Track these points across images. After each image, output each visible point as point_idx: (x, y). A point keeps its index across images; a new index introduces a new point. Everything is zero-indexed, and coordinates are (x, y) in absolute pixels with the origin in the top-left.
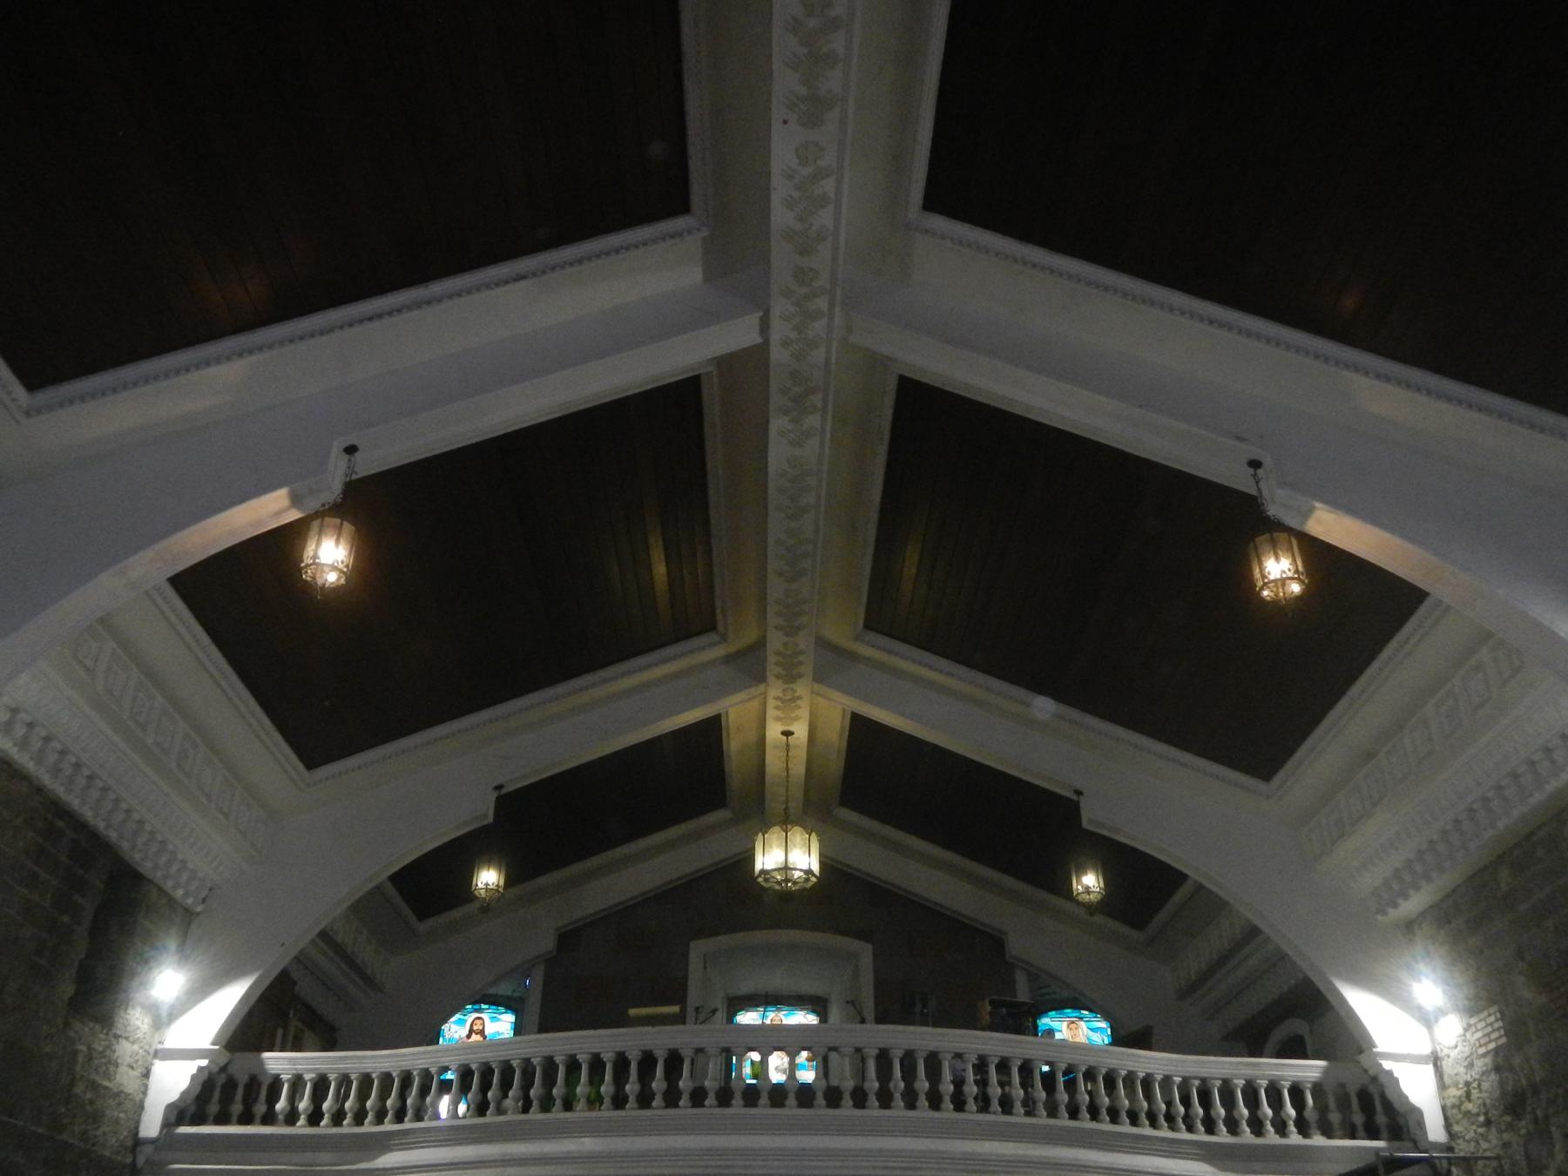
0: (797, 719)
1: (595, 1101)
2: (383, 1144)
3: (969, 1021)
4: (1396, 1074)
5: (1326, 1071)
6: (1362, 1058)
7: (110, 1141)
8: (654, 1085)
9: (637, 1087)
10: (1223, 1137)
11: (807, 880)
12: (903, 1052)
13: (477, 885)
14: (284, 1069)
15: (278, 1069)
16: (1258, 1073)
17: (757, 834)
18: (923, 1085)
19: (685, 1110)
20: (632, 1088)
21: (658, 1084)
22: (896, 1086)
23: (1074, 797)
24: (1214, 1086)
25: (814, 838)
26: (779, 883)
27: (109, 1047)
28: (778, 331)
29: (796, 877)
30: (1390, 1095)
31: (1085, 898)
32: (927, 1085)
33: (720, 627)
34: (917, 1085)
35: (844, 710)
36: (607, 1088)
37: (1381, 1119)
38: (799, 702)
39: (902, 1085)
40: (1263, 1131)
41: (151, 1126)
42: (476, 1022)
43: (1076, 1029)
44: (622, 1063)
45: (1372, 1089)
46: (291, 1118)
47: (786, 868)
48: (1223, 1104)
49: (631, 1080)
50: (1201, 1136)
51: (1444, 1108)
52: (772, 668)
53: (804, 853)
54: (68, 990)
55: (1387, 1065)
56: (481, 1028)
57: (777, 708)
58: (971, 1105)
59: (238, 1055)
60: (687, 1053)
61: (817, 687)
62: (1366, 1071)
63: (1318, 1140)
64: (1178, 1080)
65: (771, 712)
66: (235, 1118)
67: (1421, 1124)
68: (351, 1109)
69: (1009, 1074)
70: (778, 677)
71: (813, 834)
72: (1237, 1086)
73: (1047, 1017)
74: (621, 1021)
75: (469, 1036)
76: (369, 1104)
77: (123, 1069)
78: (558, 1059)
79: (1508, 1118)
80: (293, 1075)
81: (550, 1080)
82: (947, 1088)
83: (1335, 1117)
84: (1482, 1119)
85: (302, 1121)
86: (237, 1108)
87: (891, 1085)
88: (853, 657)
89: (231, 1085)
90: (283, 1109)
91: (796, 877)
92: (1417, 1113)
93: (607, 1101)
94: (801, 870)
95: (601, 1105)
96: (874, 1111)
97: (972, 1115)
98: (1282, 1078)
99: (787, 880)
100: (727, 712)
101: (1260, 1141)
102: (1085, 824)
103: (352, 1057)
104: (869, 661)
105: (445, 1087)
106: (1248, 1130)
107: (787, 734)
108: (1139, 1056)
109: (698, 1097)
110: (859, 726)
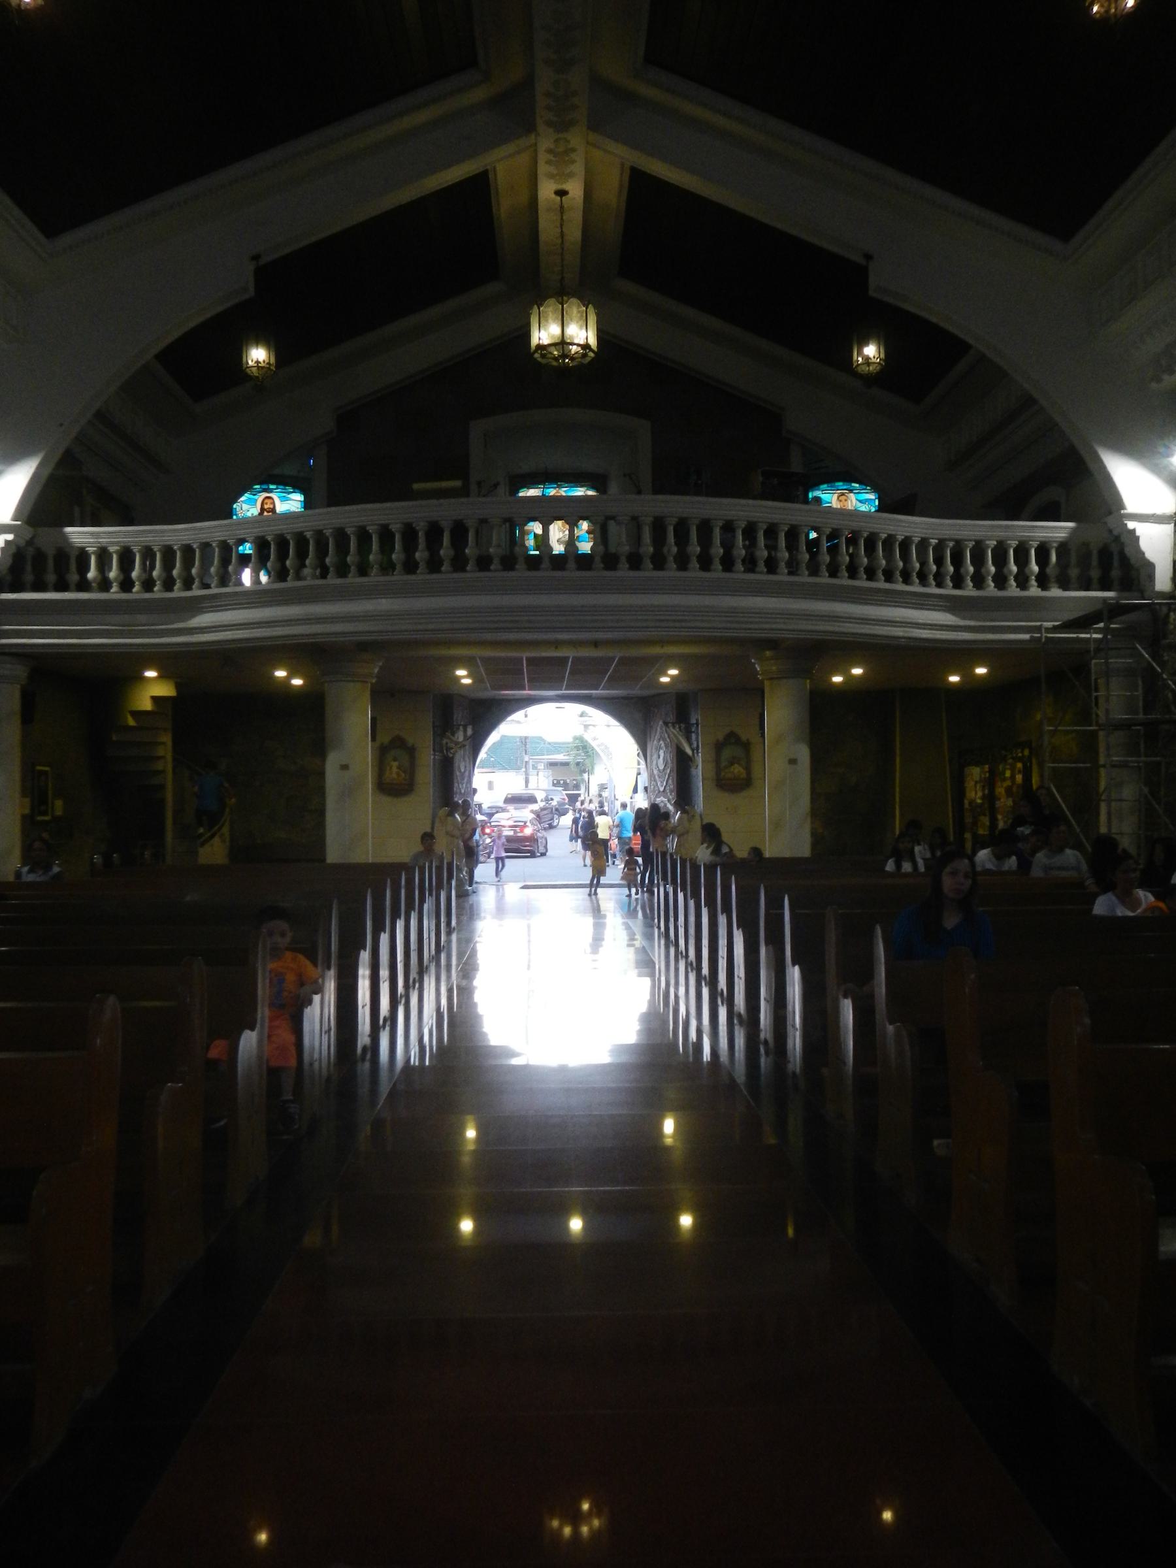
0: (571, 175)
1: (387, 567)
2: (195, 606)
3: (742, 491)
4: (1138, 533)
5: (1074, 530)
6: (1111, 521)
8: (442, 552)
9: (426, 554)
10: (969, 591)
11: (584, 356)
12: (676, 520)
13: (248, 363)
14: (89, 543)
15: (83, 543)
17: (531, 308)
18: (695, 549)
19: (471, 573)
22: (669, 551)
23: (863, 261)
24: (967, 546)
25: (591, 309)
26: (556, 359)
29: (573, 352)
30: (1128, 551)
31: (866, 369)
32: (699, 549)
35: (622, 165)
36: (397, 556)
37: (1115, 573)
38: (573, 156)
39: (675, 549)
40: (1006, 585)
42: (266, 501)
43: (846, 500)
44: (409, 534)
45: (1114, 548)
46: (105, 585)
47: (563, 343)
49: (420, 547)
50: (949, 591)
53: (581, 328)
55: (1131, 525)
56: (272, 506)
57: (548, 162)
58: (739, 567)
60: (471, 524)
61: (592, 137)
62: (1110, 531)
63: (1055, 592)
64: (934, 542)
65: (543, 168)
67: (1151, 577)
68: (159, 577)
69: (776, 539)
70: (549, 124)
71: (590, 306)
72: (988, 547)
73: (818, 490)
74: (406, 495)
75: (261, 513)
76: (175, 573)
78: (349, 531)
80: (98, 547)
82: (718, 551)
83: (1074, 572)
87: (665, 550)
89: (40, 557)
90: (95, 579)
91: (573, 352)
92: (1150, 566)
93: (399, 567)
94: (578, 345)
95: (394, 571)
96: (648, 572)
97: (739, 574)
98: (1032, 539)
99: (564, 356)
100: (495, 168)
102: (871, 293)
103: (150, 532)
105: (244, 560)
106: (992, 584)
107: (561, 193)
108: (901, 521)
109: (484, 563)
110: (639, 181)
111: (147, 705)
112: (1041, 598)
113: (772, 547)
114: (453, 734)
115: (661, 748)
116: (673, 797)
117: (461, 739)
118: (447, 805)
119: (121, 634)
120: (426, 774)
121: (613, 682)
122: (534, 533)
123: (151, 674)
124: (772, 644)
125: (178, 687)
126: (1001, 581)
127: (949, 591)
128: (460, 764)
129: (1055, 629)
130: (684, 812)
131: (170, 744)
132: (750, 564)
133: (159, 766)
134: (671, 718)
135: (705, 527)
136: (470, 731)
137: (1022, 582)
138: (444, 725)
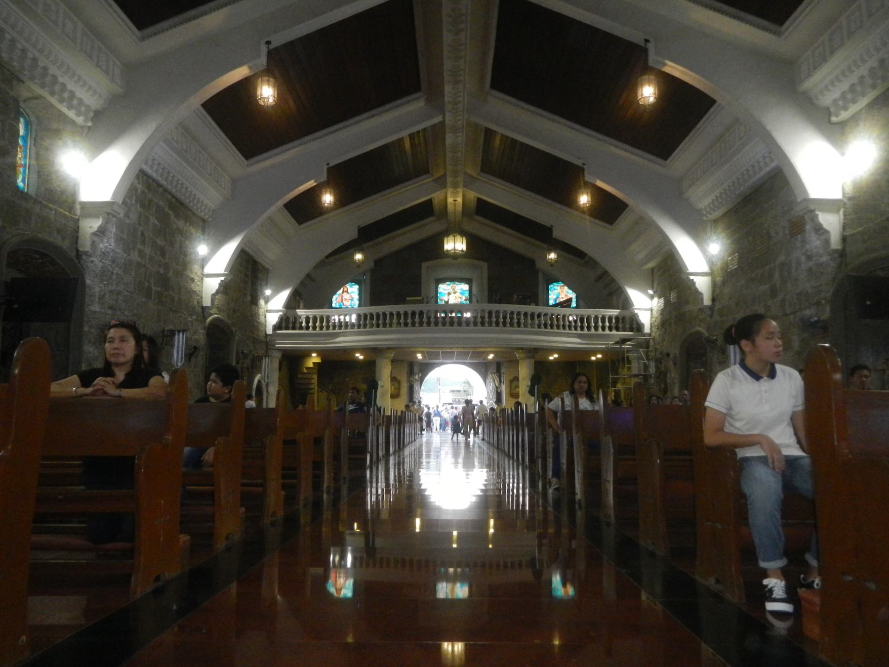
0: (458, 197)
1: (399, 324)
2: (337, 335)
5: (620, 313)
6: (630, 309)
7: (262, 335)
9: (411, 321)
10: (586, 331)
16: (600, 313)
18: (494, 319)
20: (409, 321)
21: (417, 320)
25: (464, 238)
33: (431, 172)
36: (402, 321)
37: (635, 326)
39: (488, 320)
41: (270, 331)
45: (633, 317)
48: (580, 323)
50: (579, 332)
51: (651, 324)
52: (449, 184)
54: (249, 298)
55: (636, 311)
59: (289, 310)
60: (425, 312)
61: (465, 189)
63: (614, 332)
65: (449, 195)
66: (290, 328)
67: (644, 327)
70: (451, 187)
75: (343, 293)
77: (261, 316)
79: (661, 328)
81: (385, 319)
82: (501, 320)
83: (621, 325)
84: (657, 327)
85: (311, 329)
86: (291, 325)
87: (485, 320)
88: (478, 179)
93: (402, 325)
95: (400, 325)
102: (554, 236)
104: (482, 181)
107: (455, 201)
110: (479, 200)
111: (311, 365)
113: (519, 320)
116: (495, 400)
117: (417, 378)
120: (404, 390)
121: (471, 358)
123: (314, 355)
124: (522, 349)
125: (322, 359)
127: (579, 332)
128: (416, 387)
129: (613, 344)
130: (498, 405)
131: (316, 379)
132: (512, 325)
133: (312, 386)
134: (495, 371)
135: (497, 312)
136: (420, 375)
137: (603, 328)
138: (411, 373)
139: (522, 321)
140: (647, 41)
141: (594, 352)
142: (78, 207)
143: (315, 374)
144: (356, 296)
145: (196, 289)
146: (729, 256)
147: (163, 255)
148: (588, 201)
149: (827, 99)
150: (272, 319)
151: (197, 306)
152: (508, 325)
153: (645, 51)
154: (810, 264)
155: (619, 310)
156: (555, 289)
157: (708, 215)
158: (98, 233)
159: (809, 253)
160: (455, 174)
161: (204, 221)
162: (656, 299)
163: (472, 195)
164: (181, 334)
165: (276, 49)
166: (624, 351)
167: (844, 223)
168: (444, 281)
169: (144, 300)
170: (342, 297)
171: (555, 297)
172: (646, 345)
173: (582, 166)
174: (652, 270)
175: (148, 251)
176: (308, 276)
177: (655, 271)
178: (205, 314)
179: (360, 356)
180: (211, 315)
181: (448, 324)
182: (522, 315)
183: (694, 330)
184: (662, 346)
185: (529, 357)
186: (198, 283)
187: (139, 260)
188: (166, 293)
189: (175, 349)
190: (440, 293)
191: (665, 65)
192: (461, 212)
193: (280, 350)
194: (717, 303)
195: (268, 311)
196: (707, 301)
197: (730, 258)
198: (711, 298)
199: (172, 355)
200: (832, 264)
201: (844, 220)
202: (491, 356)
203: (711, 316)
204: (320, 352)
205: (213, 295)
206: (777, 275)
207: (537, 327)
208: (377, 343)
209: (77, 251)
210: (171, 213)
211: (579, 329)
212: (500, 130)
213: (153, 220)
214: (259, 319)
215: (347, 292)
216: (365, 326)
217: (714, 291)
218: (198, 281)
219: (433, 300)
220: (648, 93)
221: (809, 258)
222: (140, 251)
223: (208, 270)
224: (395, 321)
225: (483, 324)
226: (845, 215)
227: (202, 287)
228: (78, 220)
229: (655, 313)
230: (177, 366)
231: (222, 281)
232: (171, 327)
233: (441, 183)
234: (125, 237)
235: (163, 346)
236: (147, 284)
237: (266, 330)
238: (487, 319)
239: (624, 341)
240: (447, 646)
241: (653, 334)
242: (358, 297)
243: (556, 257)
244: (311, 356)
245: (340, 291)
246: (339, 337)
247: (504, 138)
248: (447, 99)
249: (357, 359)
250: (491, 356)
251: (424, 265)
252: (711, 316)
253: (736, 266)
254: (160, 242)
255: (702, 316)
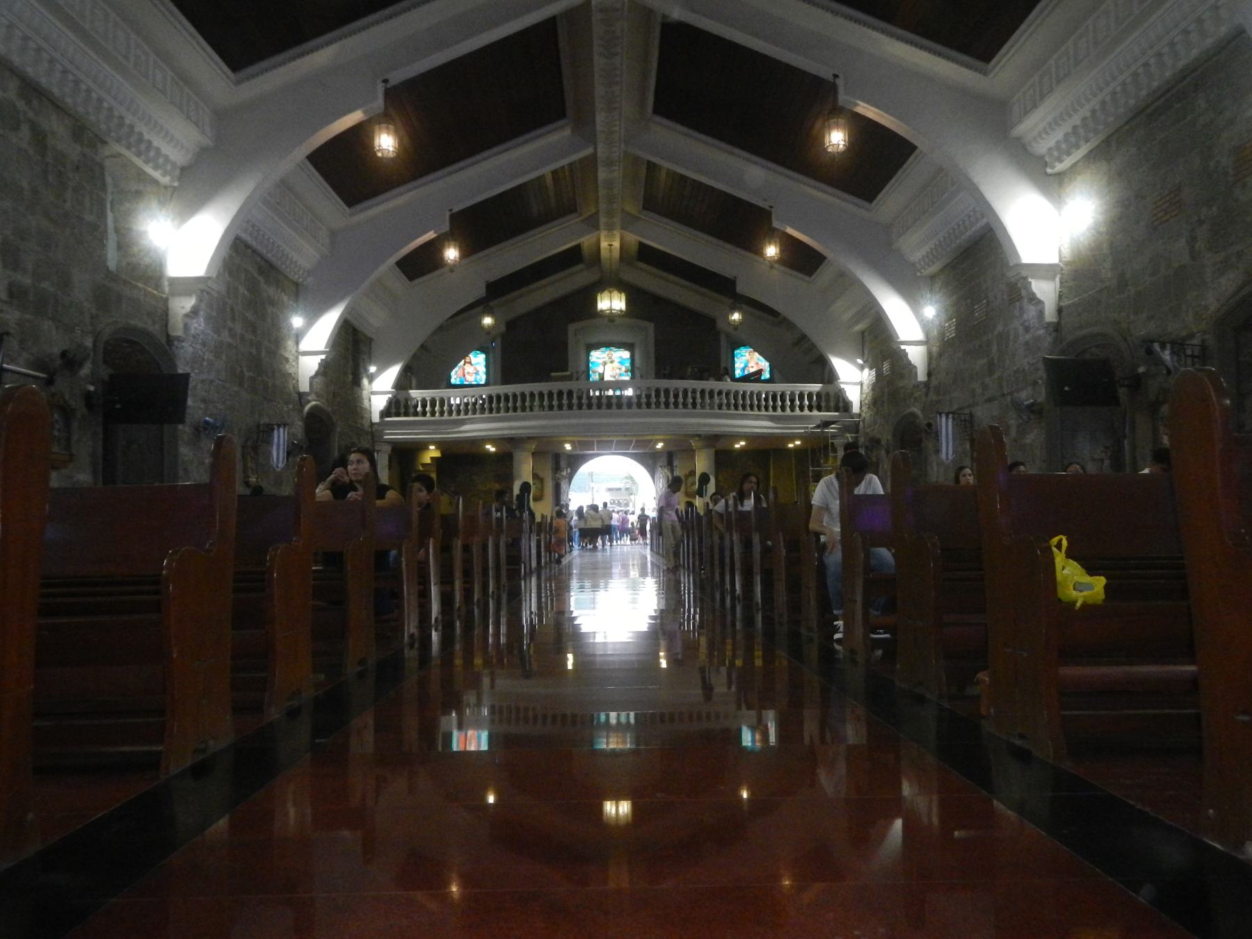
0: (615, 241)
2: (463, 422)
4: (845, 389)
5: (822, 387)
7: (367, 424)
10: (779, 412)
18: (662, 399)
20: (555, 403)
21: (565, 402)
27: (361, 393)
28: (599, 150)
33: (579, 211)
34: (660, 400)
36: (546, 403)
37: (841, 405)
41: (376, 418)
50: (771, 413)
52: (602, 226)
54: (350, 377)
55: (842, 386)
60: (575, 391)
61: (622, 231)
63: (815, 413)
65: (602, 239)
66: (402, 414)
70: (605, 229)
74: (548, 379)
75: (464, 365)
81: (524, 400)
82: (672, 400)
83: (823, 404)
85: (428, 415)
86: (402, 410)
87: (651, 400)
88: (638, 218)
92: (852, 403)
93: (546, 408)
95: (544, 408)
101: (793, 414)
104: (644, 220)
107: (611, 245)
111: (428, 461)
112: (810, 415)
113: (694, 399)
114: (561, 471)
115: (660, 478)
118: (557, 505)
119: (436, 434)
122: (599, 374)
123: (432, 447)
124: (699, 436)
125: (442, 453)
126: (792, 409)
127: (771, 413)
128: (564, 485)
129: (814, 428)
134: (665, 463)
135: (667, 391)
137: (802, 408)
138: (557, 469)
139: (699, 400)
140: (836, 76)
141: (792, 438)
142: (166, 283)
143: (433, 471)
144: (482, 369)
145: (291, 371)
146: (946, 322)
147: (254, 332)
148: (776, 254)
149: (1043, 147)
150: (378, 404)
151: (293, 392)
152: (681, 406)
153: (833, 88)
154: (1028, 337)
155: (821, 385)
156: (742, 356)
157: (922, 271)
158: (191, 315)
159: (1027, 324)
160: (610, 214)
161: (297, 284)
162: (866, 371)
163: (633, 239)
164: (281, 430)
165: (395, 87)
166: (828, 437)
167: (1060, 292)
168: (597, 346)
169: (236, 389)
170: (464, 370)
171: (742, 365)
172: (855, 428)
173: (768, 208)
174: (863, 333)
175: (238, 328)
176: (423, 347)
177: (866, 334)
178: (303, 401)
179: (491, 448)
180: (309, 402)
181: (604, 407)
182: (698, 393)
183: (908, 411)
184: (874, 430)
185: (708, 446)
186: (293, 363)
187: (230, 340)
188: (260, 378)
189: (275, 447)
190: (593, 363)
191: (857, 105)
192: (618, 259)
193: (389, 442)
194: (933, 378)
195: (373, 393)
196: (921, 376)
197: (947, 325)
198: (926, 372)
199: (270, 453)
200: (1049, 339)
201: (1060, 288)
202: (660, 446)
203: (927, 394)
204: (440, 444)
205: (312, 378)
206: (995, 348)
207: (717, 408)
208: (513, 432)
209: (168, 335)
210: (261, 279)
211: (770, 409)
212: (666, 165)
213: (242, 290)
214: (362, 403)
215: (470, 363)
216: (498, 411)
217: (929, 364)
218: (293, 361)
219: (583, 376)
220: (837, 139)
221: (1027, 329)
222: (230, 330)
223: (303, 346)
224: (536, 403)
225: (648, 405)
226: (1061, 283)
227: (298, 368)
228: (166, 300)
229: (865, 387)
230: (277, 467)
231: (322, 360)
232: (265, 420)
233: (593, 224)
234: (215, 314)
235: (260, 443)
236: (239, 369)
237: (371, 417)
238: (653, 400)
239: (826, 424)
240: (609, 807)
241: (863, 415)
242: (484, 370)
243: (741, 318)
244: (428, 449)
245: (462, 362)
246: (466, 424)
247: (670, 174)
248: (599, 128)
249: (488, 453)
250: (660, 446)
251: (572, 328)
252: (927, 394)
253: (954, 335)
254: (249, 315)
255: (917, 394)
